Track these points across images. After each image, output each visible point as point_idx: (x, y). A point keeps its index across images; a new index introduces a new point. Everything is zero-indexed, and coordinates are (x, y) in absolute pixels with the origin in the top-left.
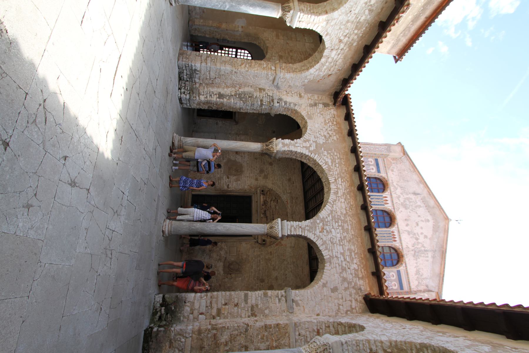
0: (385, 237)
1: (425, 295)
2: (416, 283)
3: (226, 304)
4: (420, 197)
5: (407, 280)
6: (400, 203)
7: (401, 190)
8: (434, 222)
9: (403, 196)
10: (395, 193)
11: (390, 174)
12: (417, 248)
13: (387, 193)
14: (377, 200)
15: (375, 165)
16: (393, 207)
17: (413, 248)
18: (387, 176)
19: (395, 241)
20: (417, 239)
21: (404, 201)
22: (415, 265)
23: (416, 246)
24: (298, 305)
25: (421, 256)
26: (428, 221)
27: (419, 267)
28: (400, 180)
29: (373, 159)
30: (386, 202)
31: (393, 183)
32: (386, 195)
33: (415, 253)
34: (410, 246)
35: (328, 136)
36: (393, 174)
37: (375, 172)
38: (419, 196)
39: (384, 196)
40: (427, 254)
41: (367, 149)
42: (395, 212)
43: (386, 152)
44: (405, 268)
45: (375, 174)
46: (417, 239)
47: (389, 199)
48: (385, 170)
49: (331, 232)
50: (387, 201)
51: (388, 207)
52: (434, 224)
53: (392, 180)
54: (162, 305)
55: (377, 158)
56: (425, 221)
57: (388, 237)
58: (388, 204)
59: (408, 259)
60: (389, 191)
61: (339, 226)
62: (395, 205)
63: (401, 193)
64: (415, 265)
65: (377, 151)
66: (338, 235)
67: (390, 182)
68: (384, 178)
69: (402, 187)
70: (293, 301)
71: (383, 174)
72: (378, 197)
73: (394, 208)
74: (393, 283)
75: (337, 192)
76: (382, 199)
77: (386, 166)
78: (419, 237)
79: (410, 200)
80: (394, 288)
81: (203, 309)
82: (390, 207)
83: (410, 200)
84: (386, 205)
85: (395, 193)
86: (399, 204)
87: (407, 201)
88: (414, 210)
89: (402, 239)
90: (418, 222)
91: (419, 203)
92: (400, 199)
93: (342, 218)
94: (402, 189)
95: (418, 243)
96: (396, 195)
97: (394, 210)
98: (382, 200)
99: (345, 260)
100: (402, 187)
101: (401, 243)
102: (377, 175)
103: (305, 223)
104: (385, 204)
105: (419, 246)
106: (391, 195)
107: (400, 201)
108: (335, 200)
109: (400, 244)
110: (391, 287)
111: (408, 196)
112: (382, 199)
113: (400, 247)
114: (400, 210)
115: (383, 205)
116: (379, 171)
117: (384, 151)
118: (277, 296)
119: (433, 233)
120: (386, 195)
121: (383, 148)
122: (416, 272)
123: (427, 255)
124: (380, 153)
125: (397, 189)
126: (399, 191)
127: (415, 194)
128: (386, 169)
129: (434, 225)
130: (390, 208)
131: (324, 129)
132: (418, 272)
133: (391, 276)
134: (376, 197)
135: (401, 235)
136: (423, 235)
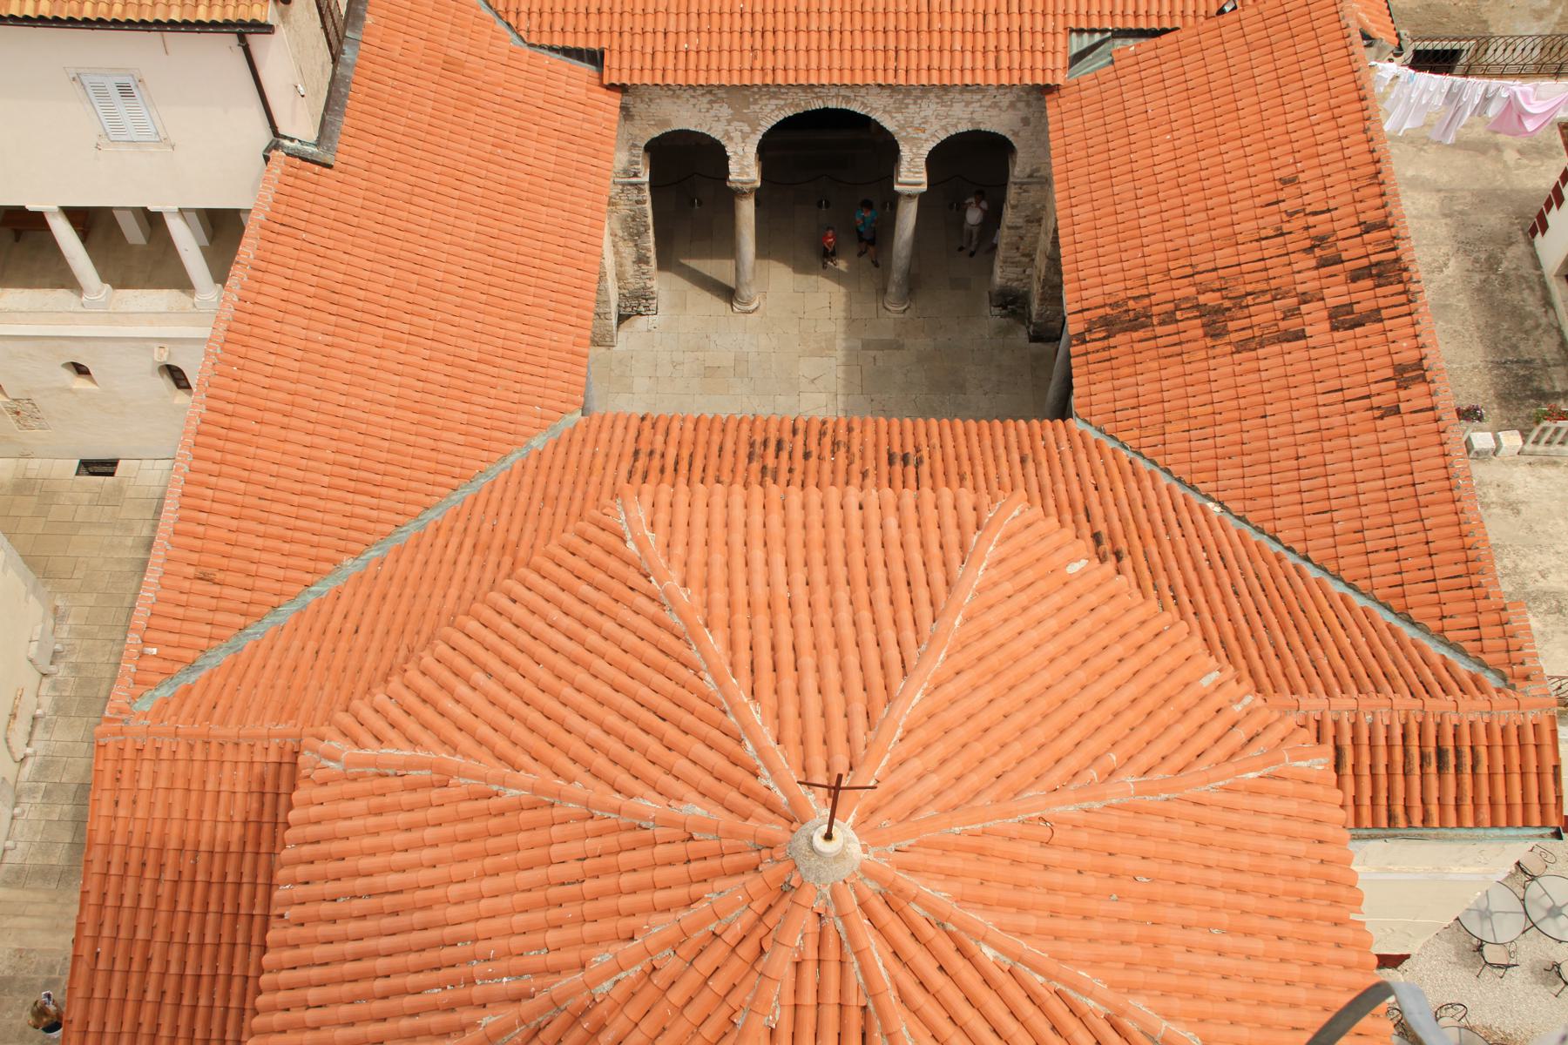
3: (1018, 249)
24: (1038, 170)
35: (709, 97)
49: (925, 117)
54: (1005, 308)
61: (915, 103)
66: (933, 106)
70: (1030, 176)
75: (844, 97)
81: (1020, 270)
93: (901, 96)
99: (979, 101)
103: (905, 151)
108: (863, 103)
118: (1019, 194)
131: (692, 101)
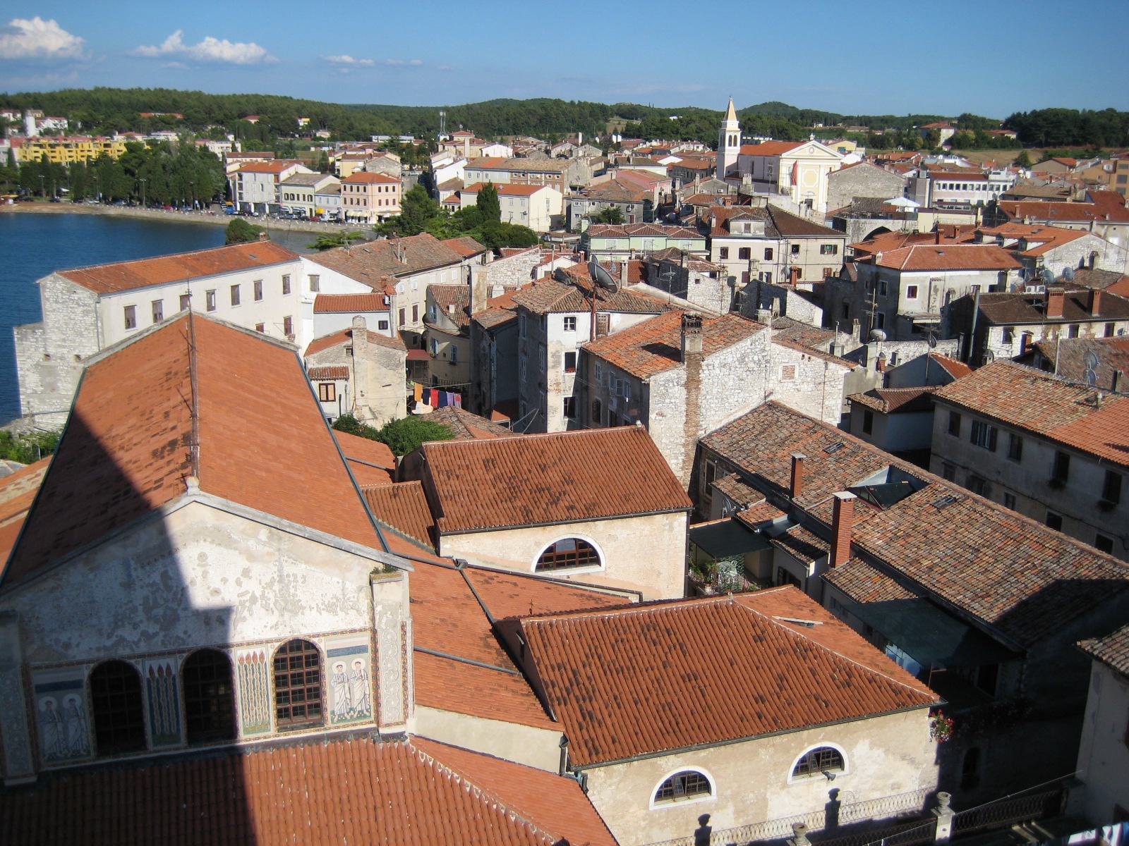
0: (254, 680)
1: (380, 612)
2: (352, 612)
4: (136, 569)
5: (349, 635)
6: (162, 634)
7: (123, 625)
8: (205, 540)
9: (141, 621)
10: (137, 643)
11: (78, 653)
12: (276, 601)
13: (139, 667)
16: (178, 655)
17: (276, 611)
18: (89, 662)
19: (262, 656)
20: (254, 600)
21: (157, 621)
22: (314, 611)
23: (272, 605)
25: (296, 595)
26: (202, 556)
27: (320, 605)
28: (94, 626)
30: (164, 669)
31: (106, 648)
32: (144, 669)
33: (289, 611)
34: (274, 619)
36: (78, 645)
38: (134, 574)
39: (148, 676)
40: (288, 576)
42: (189, 650)
44: (323, 638)
46: (254, 600)
47: (155, 663)
50: (160, 669)
51: (176, 664)
52: (209, 540)
53: (98, 649)
56: (204, 566)
57: (253, 673)
58: (168, 668)
59: (304, 626)
60: (133, 661)
62: (170, 648)
63: (134, 628)
64: (314, 611)
67: (103, 656)
69: (116, 623)
71: (85, 673)
73: (181, 652)
74: (354, 667)
77: (55, 663)
78: (247, 592)
79: (151, 602)
80: (363, 666)
83: (151, 602)
84: (174, 672)
85: (137, 643)
86: (165, 636)
87: (155, 612)
88: (179, 596)
89: (257, 637)
90: (209, 588)
91: (156, 577)
94: (120, 623)
95: (263, 596)
96: (142, 644)
97: (183, 652)
100: (116, 623)
101: (267, 642)
102: (86, 690)
104: (171, 673)
105: (271, 596)
106: (142, 656)
107: (156, 634)
109: (269, 645)
110: (362, 671)
111: (140, 608)
112: (158, 681)
113: (277, 645)
114: (182, 635)
115: (174, 679)
116: (75, 685)
119: (236, 549)
120: (144, 669)
122: (329, 612)
123: (292, 579)
125: (122, 640)
126: (128, 633)
127: (128, 585)
128: (68, 664)
129: (212, 542)
130: (180, 662)
132: (331, 608)
133: (339, 671)
134: (154, 695)
135: (247, 639)
136: (242, 579)
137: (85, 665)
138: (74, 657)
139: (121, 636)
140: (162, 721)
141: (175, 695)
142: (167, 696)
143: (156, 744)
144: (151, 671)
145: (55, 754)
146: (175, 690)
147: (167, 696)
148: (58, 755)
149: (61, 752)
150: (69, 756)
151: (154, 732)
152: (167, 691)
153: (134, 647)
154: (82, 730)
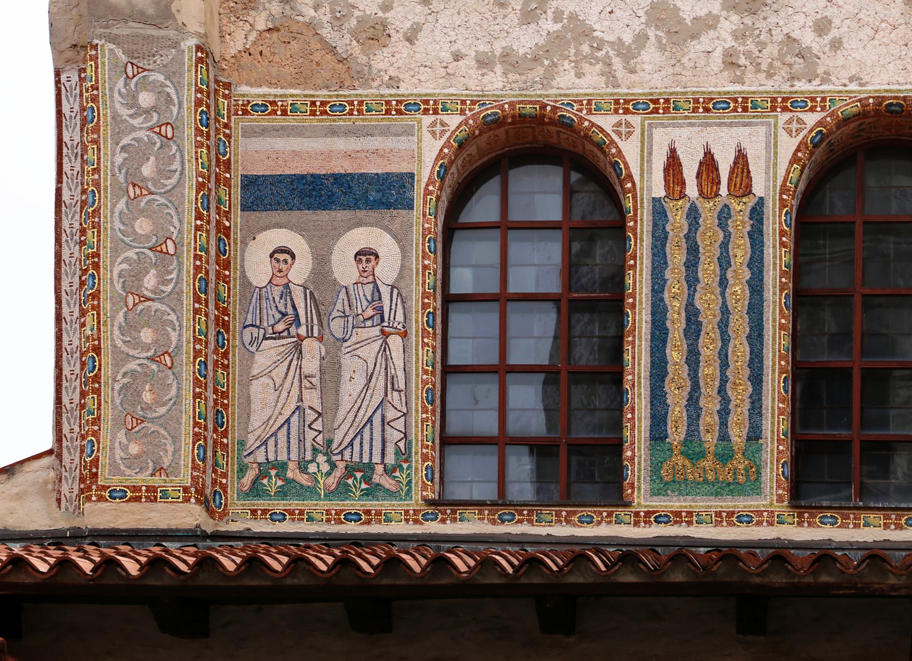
10: (628, 54)
13: (630, 150)
14: (708, 270)
15: (323, 216)
16: (784, 117)
29: (251, 234)
36: (410, 39)
37: (401, 239)
39: (659, 191)
41: (150, 281)
43: (173, 74)
45: (416, 235)
48: (374, 120)
50: (708, 164)
55: (237, 182)
58: (741, 159)
60: (606, 122)
65: (163, 172)
68: (461, 145)
72: (677, 257)
76: (693, 214)
82: (772, 146)
84: (759, 189)
85: (628, 54)
92: (688, 18)
98: (708, 211)
104: (748, 191)
112: (693, 214)
115: (757, 213)
117: (159, 90)
121: (131, 100)
124: (189, 147)
130: (788, 146)
137: (428, 120)
138: (394, 82)
139: (573, 17)
140: (695, 387)
141: (756, 286)
142: (723, 283)
143: (660, 488)
144: (673, 165)
145: (282, 467)
146: (756, 263)
147: (723, 283)
148: (292, 472)
149: (303, 467)
150: (332, 481)
151: (658, 434)
152: (724, 262)
153: (617, 63)
154: (391, 384)
